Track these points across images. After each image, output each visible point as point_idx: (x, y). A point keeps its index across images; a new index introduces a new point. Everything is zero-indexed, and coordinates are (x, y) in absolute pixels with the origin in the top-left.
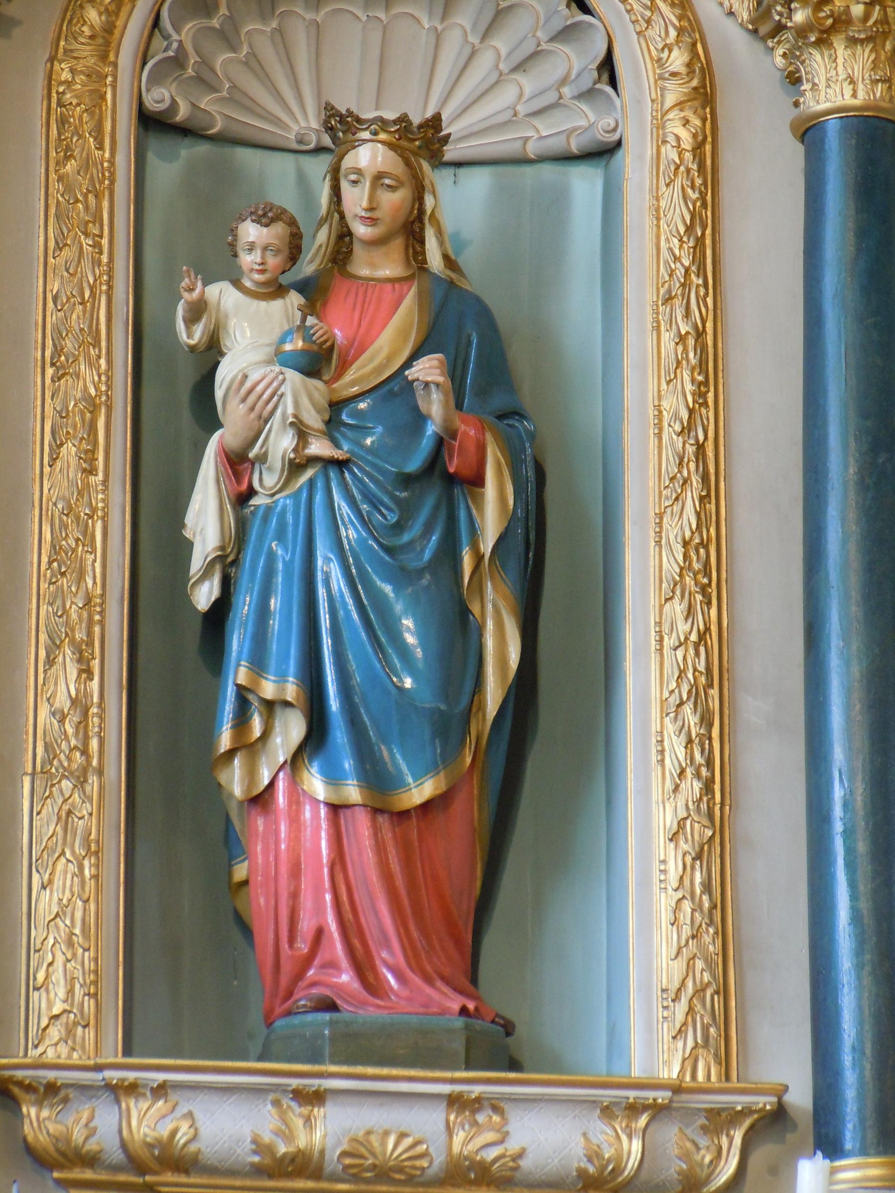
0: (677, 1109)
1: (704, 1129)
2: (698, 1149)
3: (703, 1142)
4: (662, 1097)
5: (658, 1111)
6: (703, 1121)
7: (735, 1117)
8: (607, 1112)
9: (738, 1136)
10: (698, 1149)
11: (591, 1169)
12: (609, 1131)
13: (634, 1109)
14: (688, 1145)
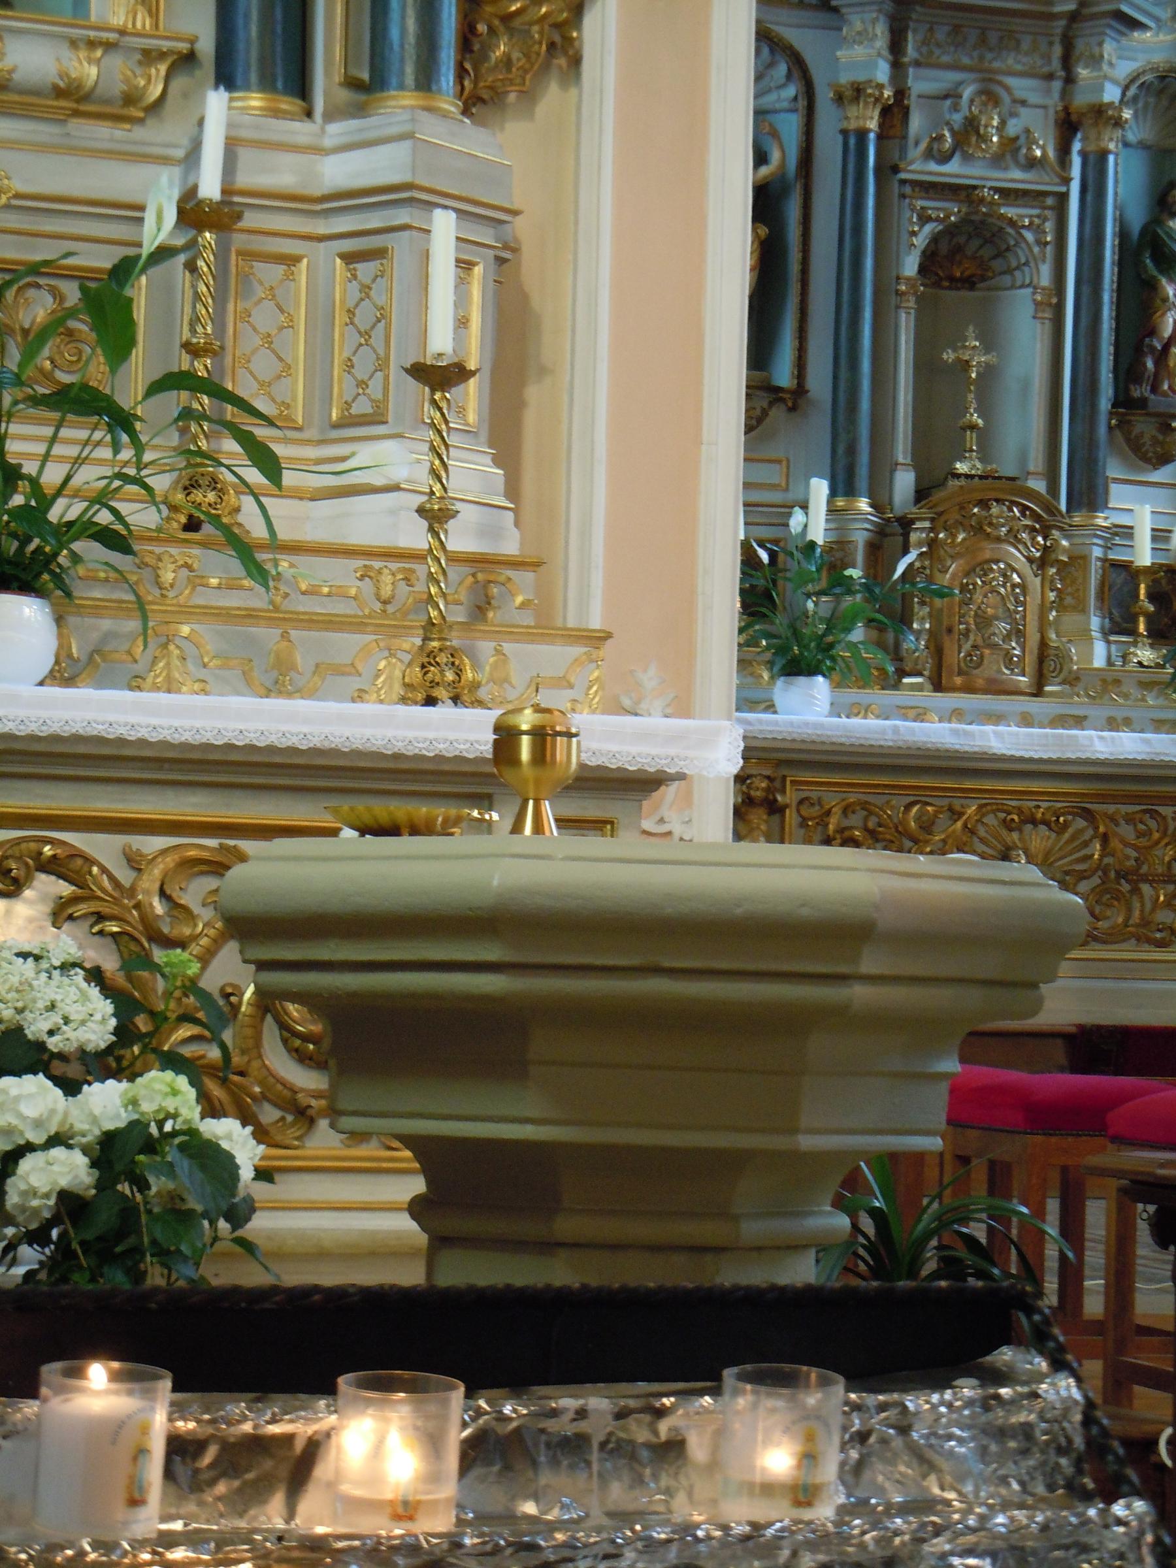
0: (123, 47)
1: (140, 63)
2: (135, 76)
3: (138, 71)
4: (112, 37)
5: (109, 46)
6: (138, 57)
7: (162, 55)
8: (74, 44)
9: (163, 68)
10: (135, 76)
11: (62, 84)
12: (74, 58)
13: (92, 44)
14: (129, 73)
